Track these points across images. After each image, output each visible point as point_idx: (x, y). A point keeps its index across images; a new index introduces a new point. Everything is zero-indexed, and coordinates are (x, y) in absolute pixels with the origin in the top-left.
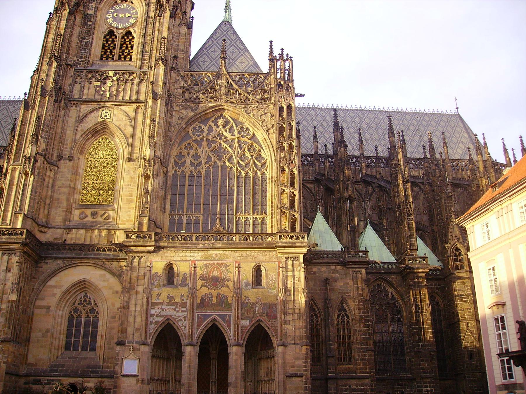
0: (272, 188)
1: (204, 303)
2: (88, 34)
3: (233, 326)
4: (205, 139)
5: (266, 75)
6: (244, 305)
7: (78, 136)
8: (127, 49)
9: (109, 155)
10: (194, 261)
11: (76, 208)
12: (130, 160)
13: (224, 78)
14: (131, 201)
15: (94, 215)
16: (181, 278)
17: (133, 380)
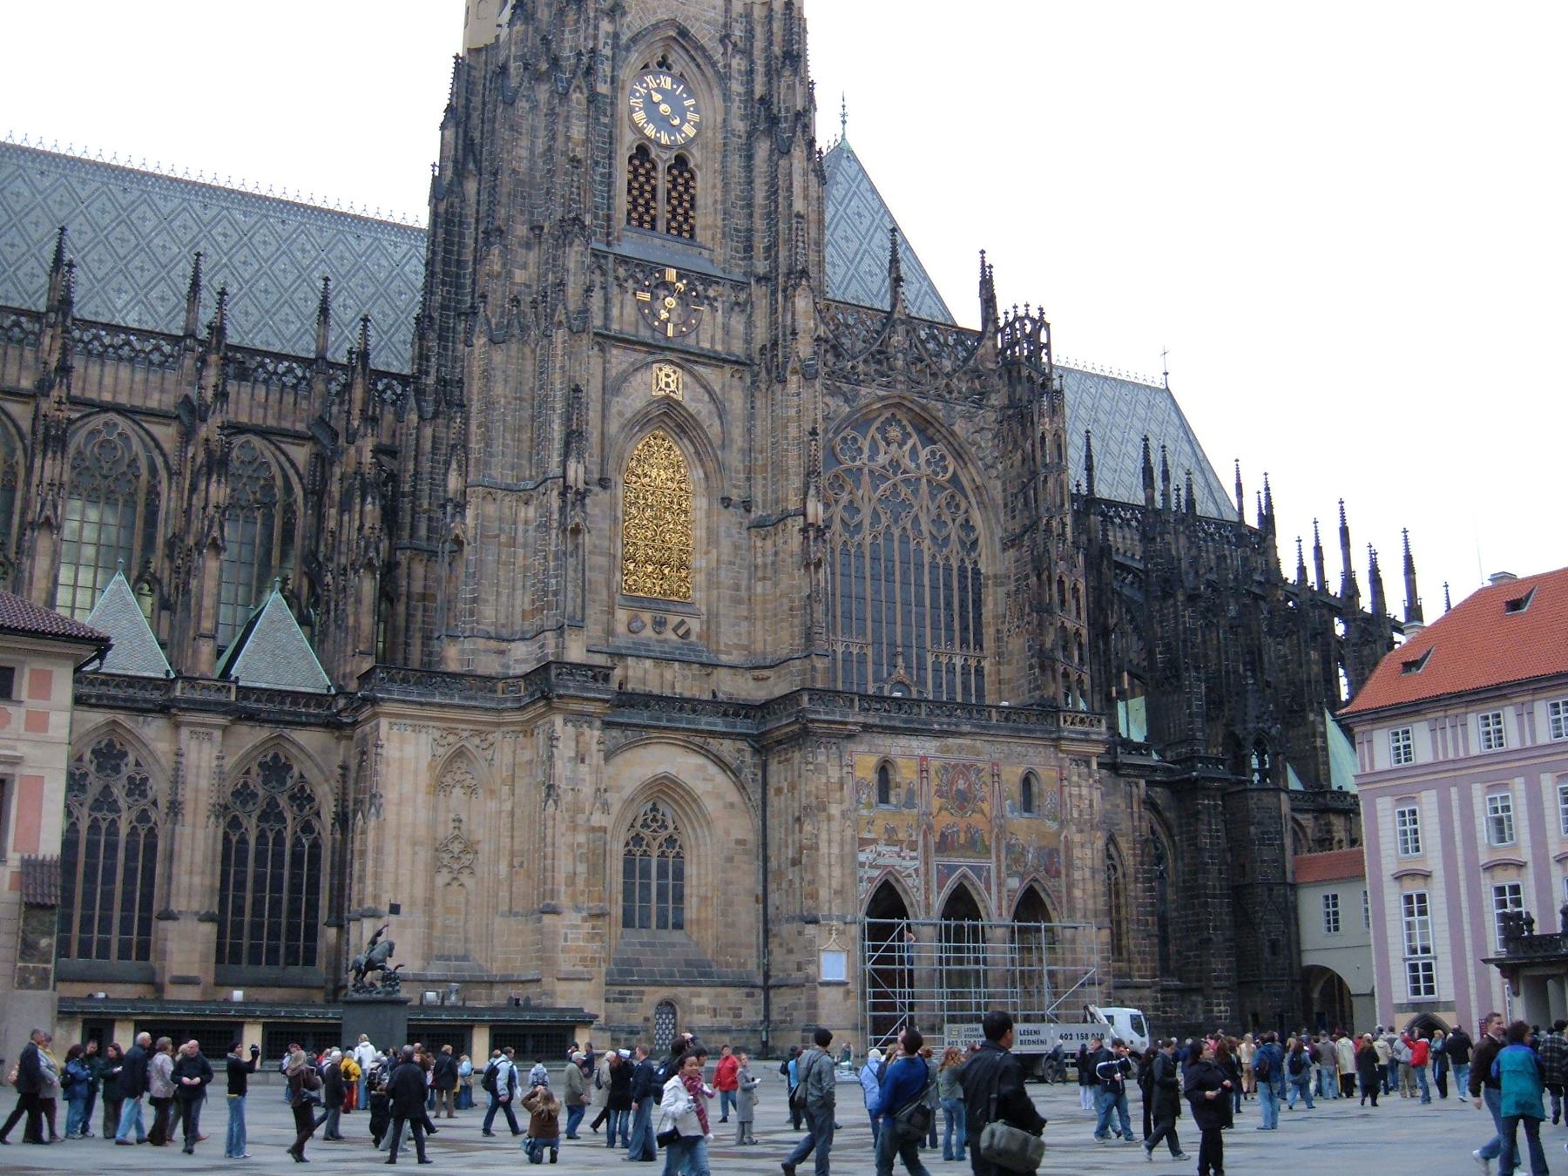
0: (995, 600)
1: (945, 844)
2: (603, 150)
3: (994, 889)
4: (866, 471)
5: (980, 336)
6: (1009, 847)
7: (613, 427)
8: (680, 204)
9: (672, 480)
10: (924, 758)
11: (622, 607)
12: (726, 502)
13: (901, 329)
14: (737, 601)
15: (659, 624)
16: (902, 792)
17: (835, 994)
